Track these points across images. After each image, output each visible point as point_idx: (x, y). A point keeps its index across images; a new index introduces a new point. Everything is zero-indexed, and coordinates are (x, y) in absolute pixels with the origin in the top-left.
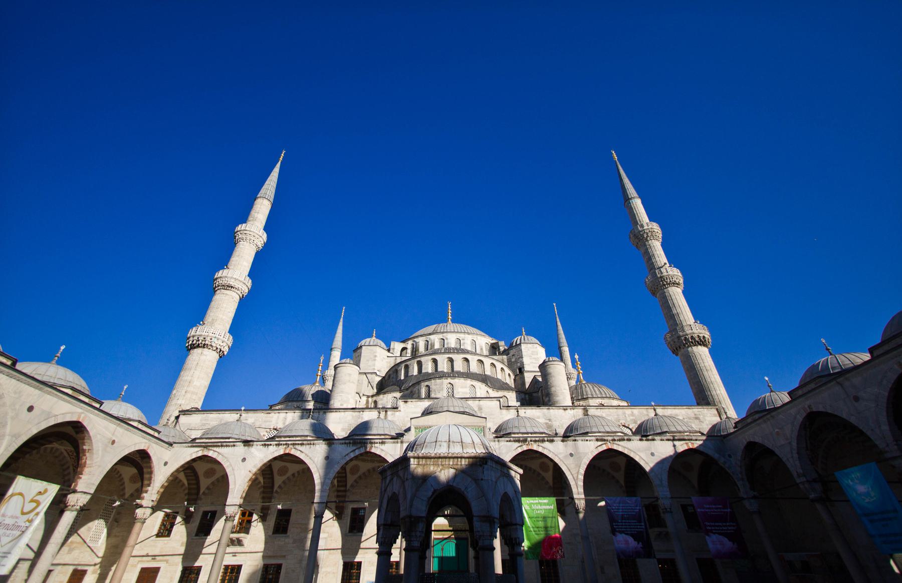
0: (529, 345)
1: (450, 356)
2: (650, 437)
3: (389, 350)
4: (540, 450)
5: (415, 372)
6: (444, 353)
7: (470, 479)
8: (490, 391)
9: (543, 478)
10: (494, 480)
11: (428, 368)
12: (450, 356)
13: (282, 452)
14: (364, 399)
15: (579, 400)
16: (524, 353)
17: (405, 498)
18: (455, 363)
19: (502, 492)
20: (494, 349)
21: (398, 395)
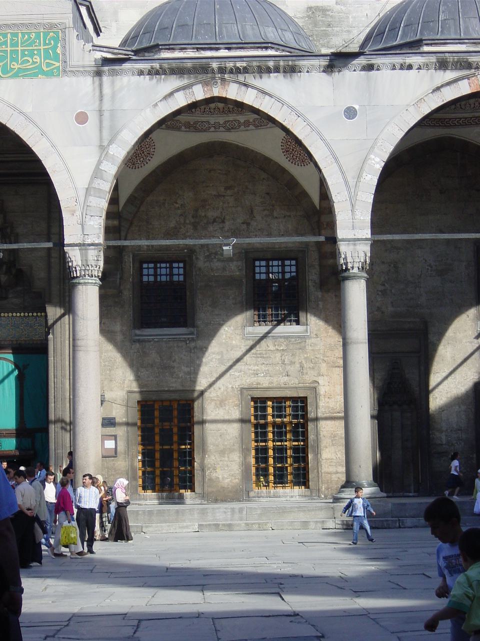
4: (249, 98)
9: (292, 183)
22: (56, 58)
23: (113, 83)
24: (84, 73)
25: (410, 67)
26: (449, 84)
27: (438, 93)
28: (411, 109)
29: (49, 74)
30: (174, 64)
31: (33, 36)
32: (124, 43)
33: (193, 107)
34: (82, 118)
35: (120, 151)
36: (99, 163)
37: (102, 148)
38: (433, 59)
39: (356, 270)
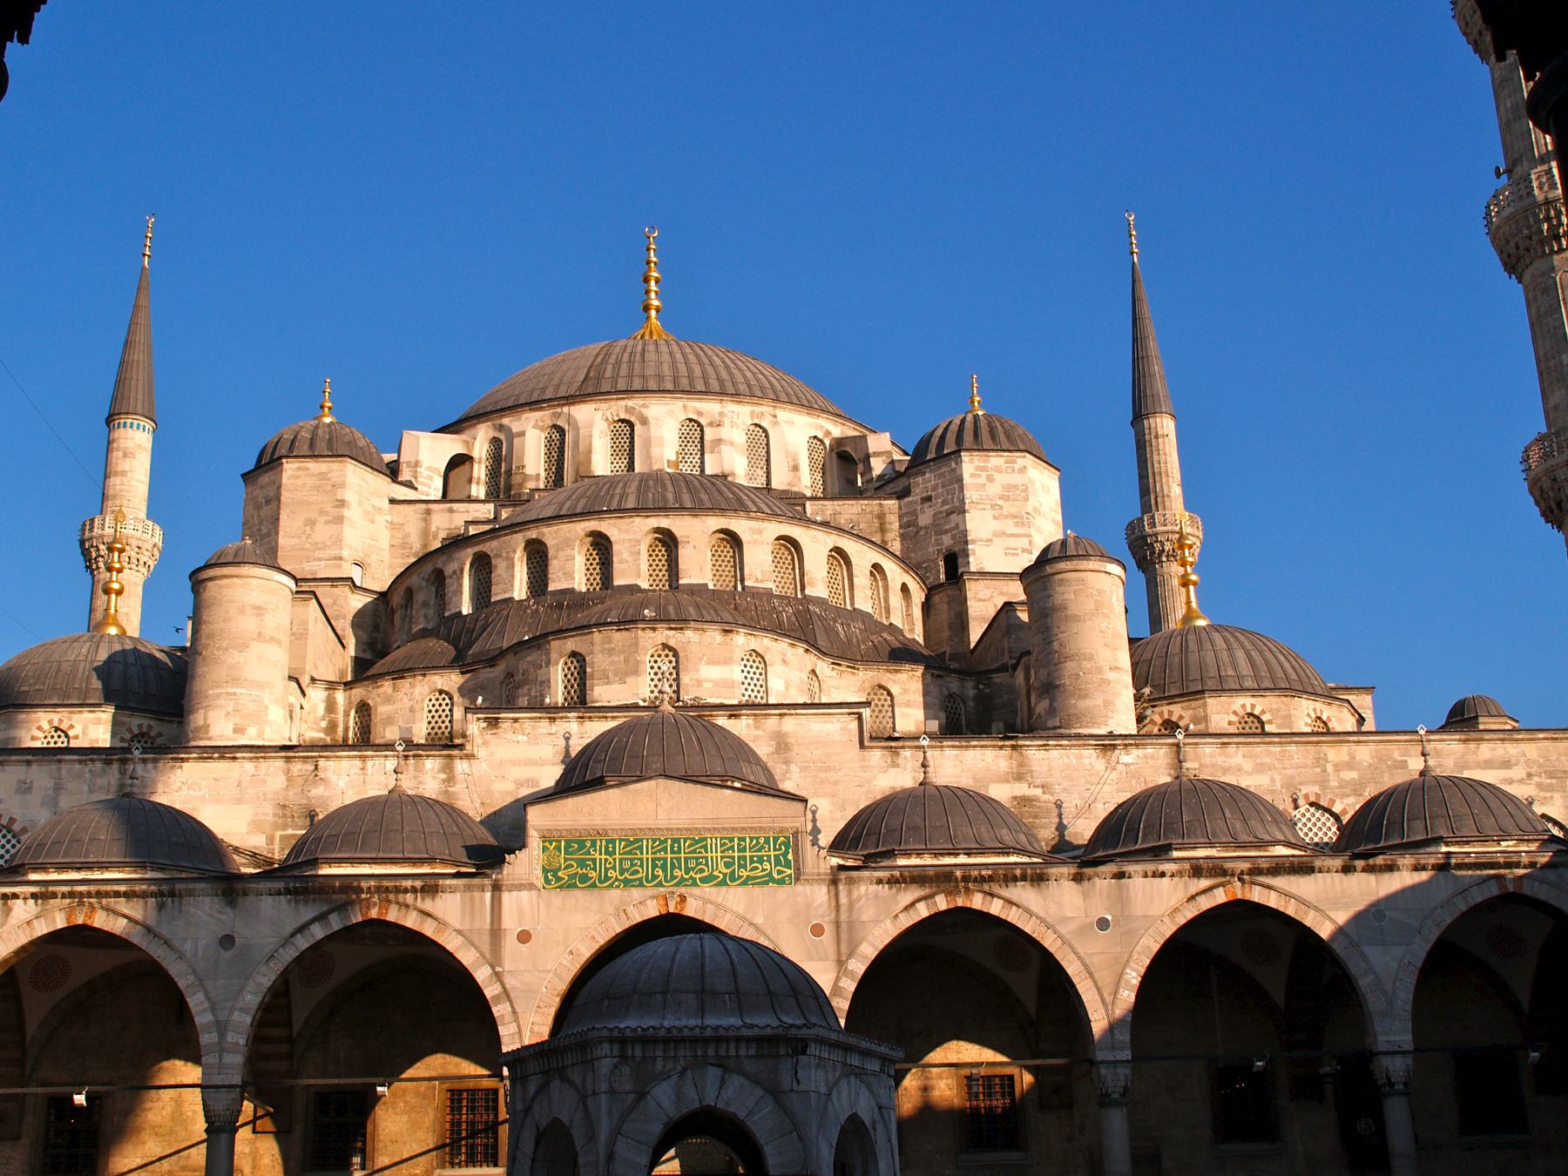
0: (996, 460)
1: (664, 522)
2: (1380, 860)
3: (393, 471)
4: (995, 908)
5: (519, 589)
6: (641, 510)
7: (759, 1092)
8: (824, 667)
10: (823, 1090)
11: (573, 571)
12: (664, 522)
13: (60, 923)
14: (317, 695)
15: (1171, 700)
16: (970, 495)
17: (591, 1136)
18: (685, 555)
19: (844, 1117)
20: (843, 464)
21: (452, 680)
22: (788, 865)
23: (850, 893)
24: (819, 881)
25: (1163, 875)
26: (1204, 892)
27: (1193, 903)
28: (1166, 919)
29: (781, 882)
30: (916, 872)
31: (762, 841)
32: (840, 844)
33: (936, 919)
34: (817, 930)
35: (859, 967)
36: (838, 979)
37: (841, 963)
38: (1187, 866)
39: (1116, 1096)
